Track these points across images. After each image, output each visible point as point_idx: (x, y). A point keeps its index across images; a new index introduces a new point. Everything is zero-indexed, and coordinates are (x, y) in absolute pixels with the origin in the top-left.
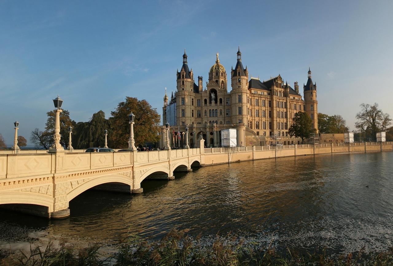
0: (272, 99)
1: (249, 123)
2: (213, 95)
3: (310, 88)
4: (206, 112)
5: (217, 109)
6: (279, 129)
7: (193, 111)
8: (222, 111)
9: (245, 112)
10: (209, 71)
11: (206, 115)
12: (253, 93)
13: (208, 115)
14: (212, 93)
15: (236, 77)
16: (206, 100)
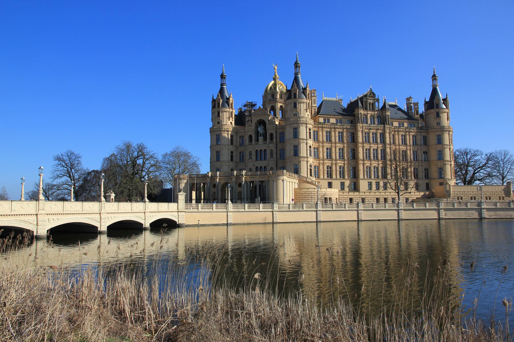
0: (355, 128)
1: (311, 170)
2: (259, 129)
3: (435, 105)
4: (250, 154)
5: (265, 148)
6: (370, 177)
7: (232, 152)
8: (273, 152)
9: (303, 151)
10: (263, 93)
11: (250, 158)
12: (333, 123)
13: (254, 157)
14: (260, 125)
15: (290, 101)
16: (251, 137)
